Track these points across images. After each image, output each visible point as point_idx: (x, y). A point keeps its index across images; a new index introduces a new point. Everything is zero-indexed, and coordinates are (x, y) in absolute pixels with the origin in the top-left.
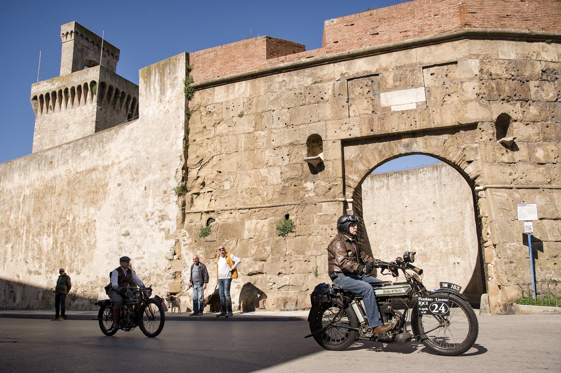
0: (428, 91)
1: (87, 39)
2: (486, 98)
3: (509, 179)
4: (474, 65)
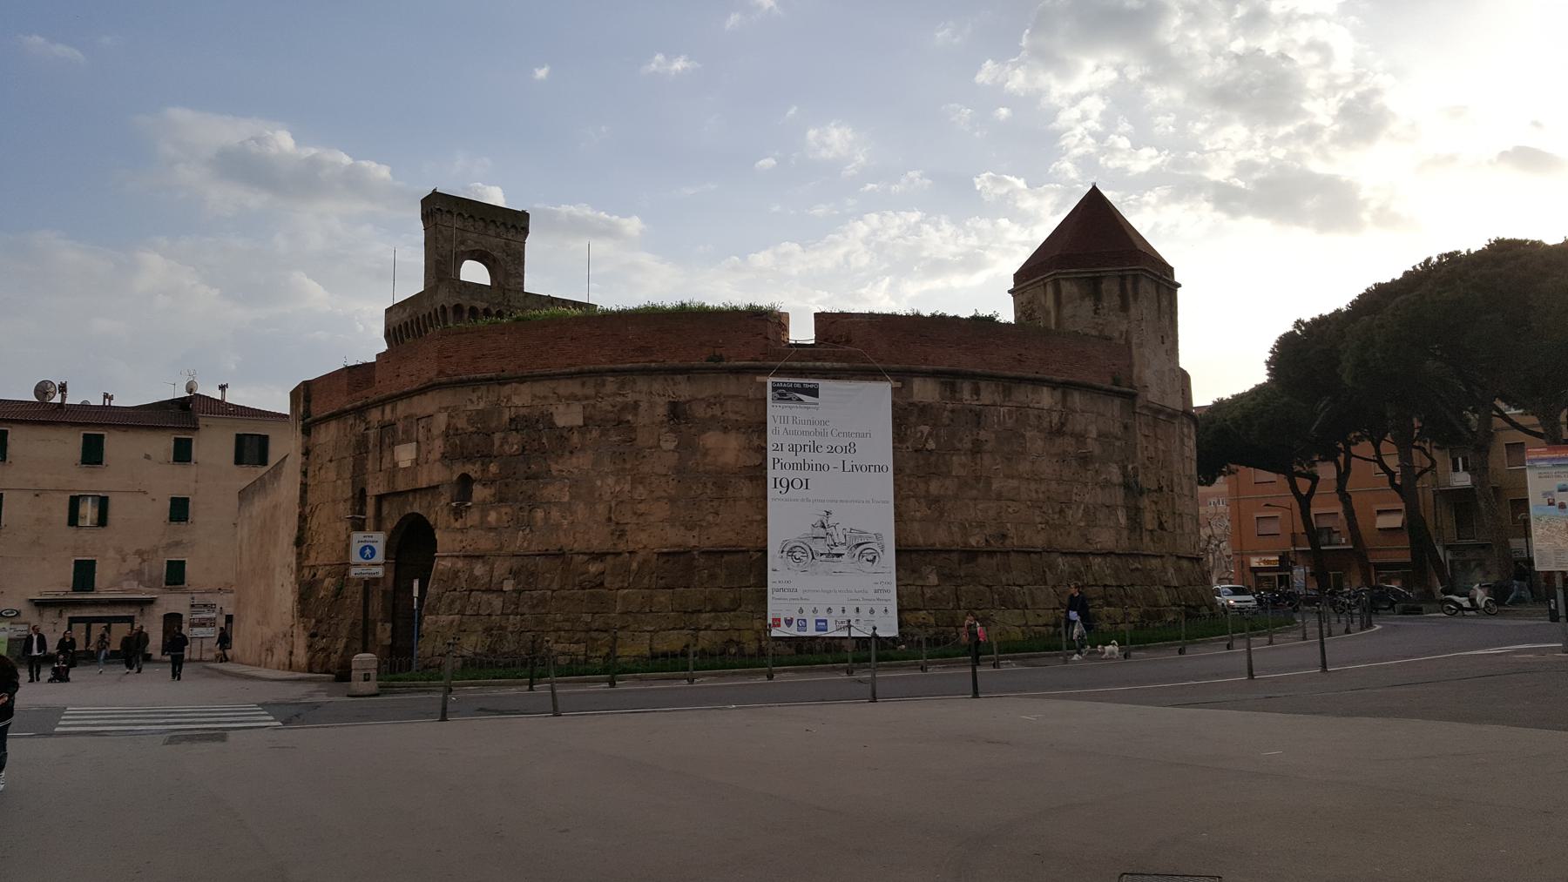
0: (418, 449)
1: (460, 214)
2: (448, 458)
3: (458, 547)
4: (441, 420)
